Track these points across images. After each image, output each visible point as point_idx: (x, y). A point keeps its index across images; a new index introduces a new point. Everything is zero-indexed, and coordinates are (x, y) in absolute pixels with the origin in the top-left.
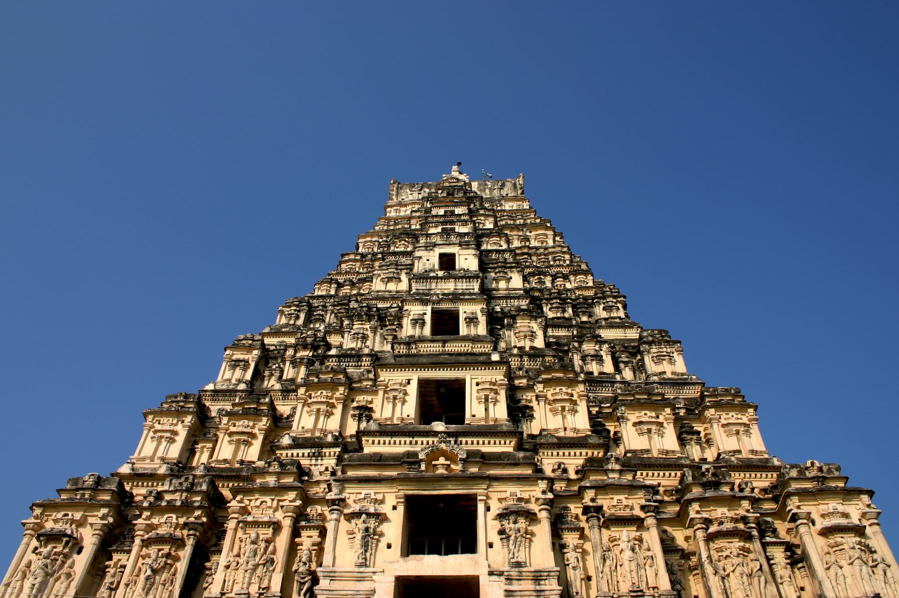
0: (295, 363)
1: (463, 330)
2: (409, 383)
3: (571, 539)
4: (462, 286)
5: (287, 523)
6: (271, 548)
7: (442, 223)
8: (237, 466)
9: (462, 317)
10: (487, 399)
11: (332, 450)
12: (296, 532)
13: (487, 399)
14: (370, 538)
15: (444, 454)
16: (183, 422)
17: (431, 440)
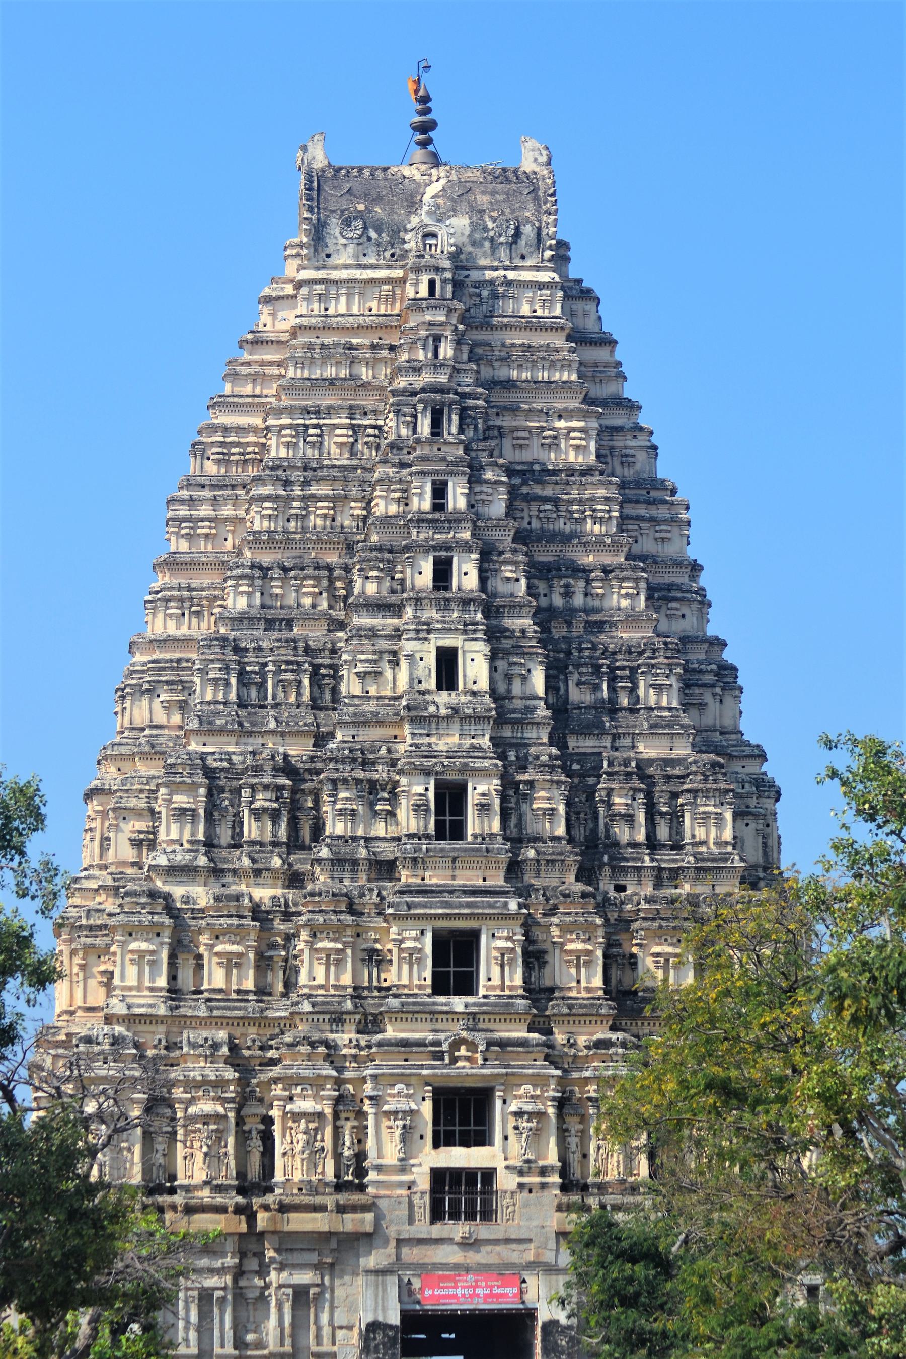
0: (257, 814)
1: (473, 824)
2: (422, 933)
3: (574, 1124)
4: (473, 729)
5: (328, 1111)
6: (319, 1137)
7: (435, 548)
8: (234, 996)
9: (472, 798)
10: (503, 955)
11: (351, 1016)
12: (336, 1115)
13: (503, 955)
14: (407, 1134)
15: (463, 1041)
16: (158, 935)
17: (450, 1017)
